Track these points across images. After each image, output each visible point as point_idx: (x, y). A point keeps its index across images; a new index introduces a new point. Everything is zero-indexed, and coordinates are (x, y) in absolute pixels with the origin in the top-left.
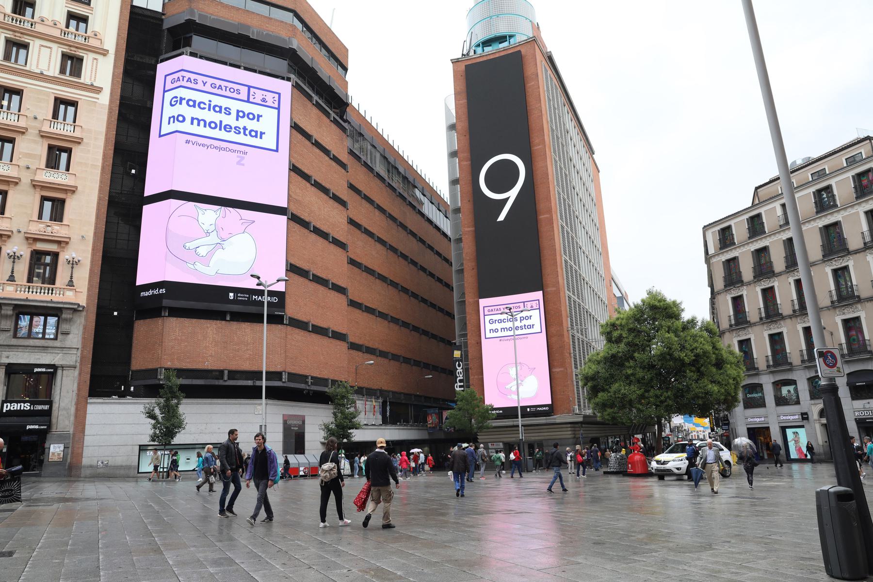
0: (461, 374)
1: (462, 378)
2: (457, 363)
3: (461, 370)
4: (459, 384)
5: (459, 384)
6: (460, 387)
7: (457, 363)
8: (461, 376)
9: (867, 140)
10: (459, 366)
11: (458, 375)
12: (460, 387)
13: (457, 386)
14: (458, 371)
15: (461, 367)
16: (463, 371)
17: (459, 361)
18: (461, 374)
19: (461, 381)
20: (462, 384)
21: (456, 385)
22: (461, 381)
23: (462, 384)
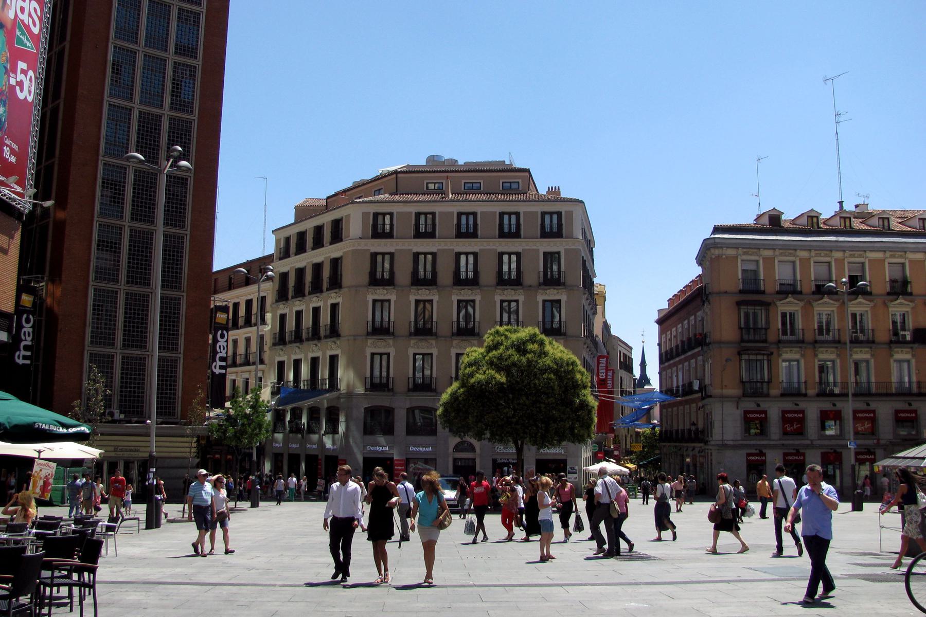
0: (29, 336)
1: (30, 343)
2: (25, 316)
3: (31, 330)
4: (23, 353)
5: (23, 353)
6: (25, 357)
7: (25, 316)
8: (30, 339)
9: (526, 172)
10: (28, 321)
11: (23, 337)
12: (25, 357)
13: (19, 357)
14: (23, 330)
15: (31, 324)
16: (33, 332)
17: (29, 312)
18: (29, 336)
19: (26, 348)
20: (28, 353)
21: (17, 353)
22: (26, 348)
23: (28, 353)
